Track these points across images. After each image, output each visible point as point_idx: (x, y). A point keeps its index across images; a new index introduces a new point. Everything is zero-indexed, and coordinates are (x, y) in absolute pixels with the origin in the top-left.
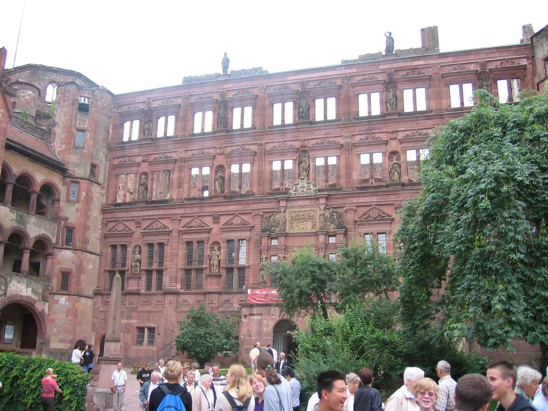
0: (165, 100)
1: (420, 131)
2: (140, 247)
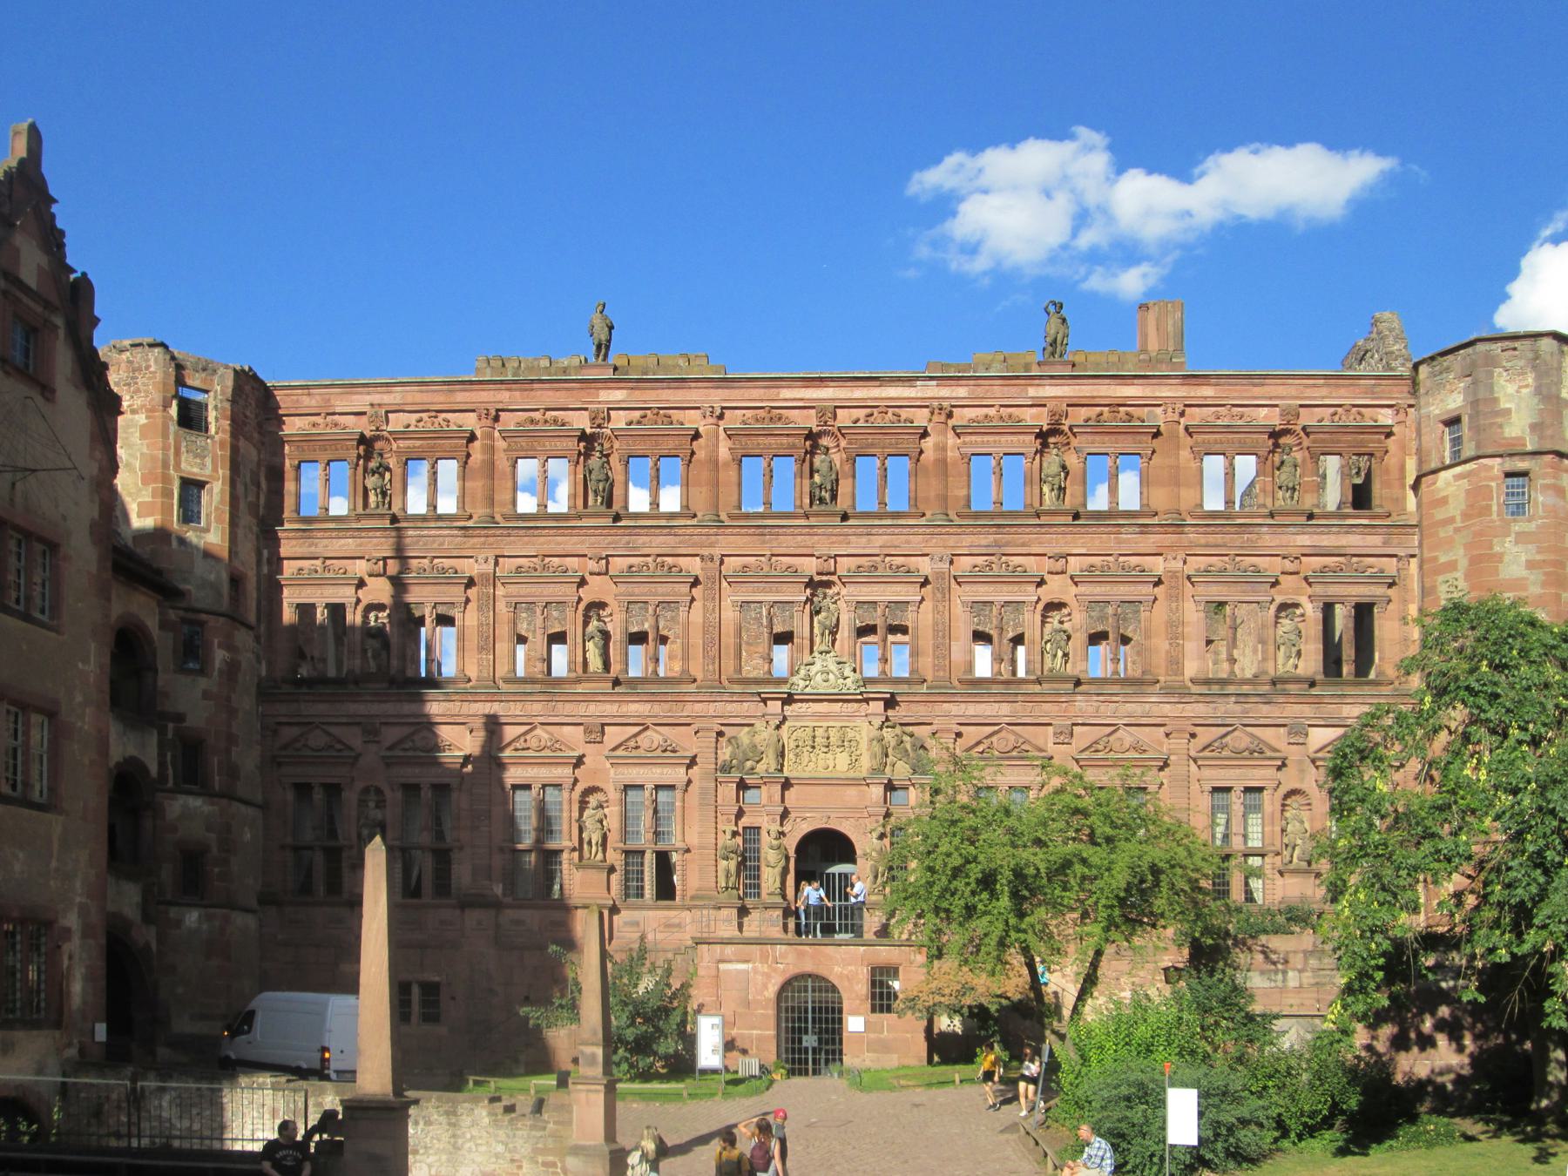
0: (424, 415)
1: (1122, 559)
2: (379, 791)
